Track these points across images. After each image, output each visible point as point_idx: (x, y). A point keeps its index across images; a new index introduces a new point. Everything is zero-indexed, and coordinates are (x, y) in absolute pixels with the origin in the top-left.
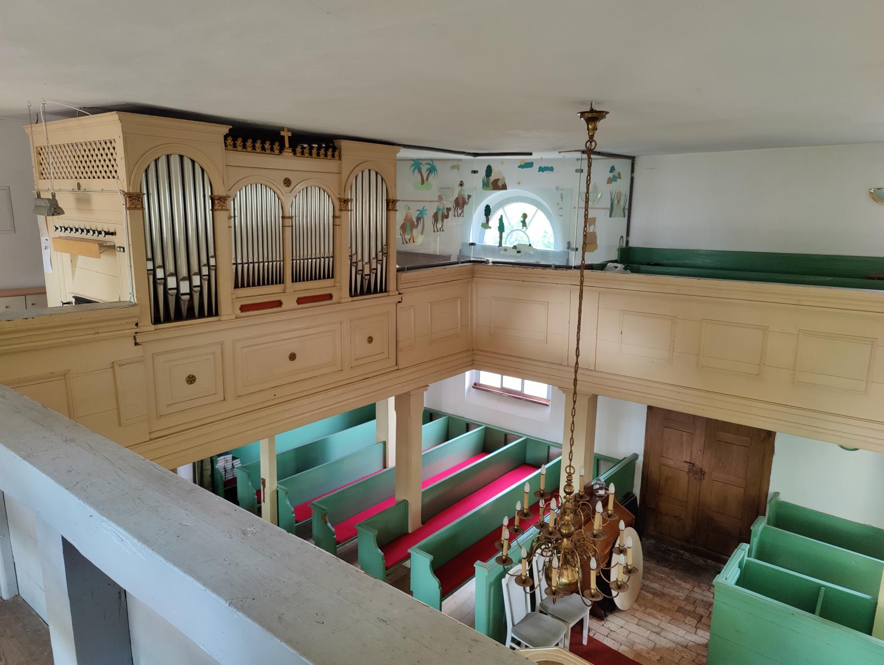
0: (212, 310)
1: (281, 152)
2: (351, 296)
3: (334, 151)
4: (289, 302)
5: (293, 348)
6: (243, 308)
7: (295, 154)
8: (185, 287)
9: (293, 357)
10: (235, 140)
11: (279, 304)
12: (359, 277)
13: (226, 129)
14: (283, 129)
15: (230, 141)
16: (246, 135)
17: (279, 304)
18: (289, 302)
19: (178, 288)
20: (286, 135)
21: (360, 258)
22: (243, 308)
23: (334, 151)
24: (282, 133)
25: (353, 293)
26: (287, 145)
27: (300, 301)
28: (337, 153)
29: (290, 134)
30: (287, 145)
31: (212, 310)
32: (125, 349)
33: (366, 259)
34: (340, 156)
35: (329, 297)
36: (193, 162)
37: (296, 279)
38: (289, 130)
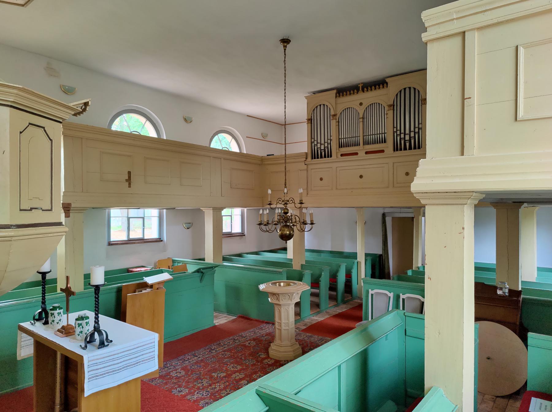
2: (394, 151)
3: (383, 85)
4: (362, 154)
5: (361, 172)
7: (364, 92)
8: (322, 148)
9: (361, 177)
12: (403, 142)
13: (335, 91)
14: (359, 84)
15: (338, 95)
16: (341, 91)
17: (356, 154)
18: (362, 154)
20: (360, 86)
21: (402, 131)
22: (342, 155)
23: (383, 85)
25: (396, 148)
27: (367, 153)
28: (385, 85)
33: (407, 132)
35: (382, 151)
37: (366, 143)
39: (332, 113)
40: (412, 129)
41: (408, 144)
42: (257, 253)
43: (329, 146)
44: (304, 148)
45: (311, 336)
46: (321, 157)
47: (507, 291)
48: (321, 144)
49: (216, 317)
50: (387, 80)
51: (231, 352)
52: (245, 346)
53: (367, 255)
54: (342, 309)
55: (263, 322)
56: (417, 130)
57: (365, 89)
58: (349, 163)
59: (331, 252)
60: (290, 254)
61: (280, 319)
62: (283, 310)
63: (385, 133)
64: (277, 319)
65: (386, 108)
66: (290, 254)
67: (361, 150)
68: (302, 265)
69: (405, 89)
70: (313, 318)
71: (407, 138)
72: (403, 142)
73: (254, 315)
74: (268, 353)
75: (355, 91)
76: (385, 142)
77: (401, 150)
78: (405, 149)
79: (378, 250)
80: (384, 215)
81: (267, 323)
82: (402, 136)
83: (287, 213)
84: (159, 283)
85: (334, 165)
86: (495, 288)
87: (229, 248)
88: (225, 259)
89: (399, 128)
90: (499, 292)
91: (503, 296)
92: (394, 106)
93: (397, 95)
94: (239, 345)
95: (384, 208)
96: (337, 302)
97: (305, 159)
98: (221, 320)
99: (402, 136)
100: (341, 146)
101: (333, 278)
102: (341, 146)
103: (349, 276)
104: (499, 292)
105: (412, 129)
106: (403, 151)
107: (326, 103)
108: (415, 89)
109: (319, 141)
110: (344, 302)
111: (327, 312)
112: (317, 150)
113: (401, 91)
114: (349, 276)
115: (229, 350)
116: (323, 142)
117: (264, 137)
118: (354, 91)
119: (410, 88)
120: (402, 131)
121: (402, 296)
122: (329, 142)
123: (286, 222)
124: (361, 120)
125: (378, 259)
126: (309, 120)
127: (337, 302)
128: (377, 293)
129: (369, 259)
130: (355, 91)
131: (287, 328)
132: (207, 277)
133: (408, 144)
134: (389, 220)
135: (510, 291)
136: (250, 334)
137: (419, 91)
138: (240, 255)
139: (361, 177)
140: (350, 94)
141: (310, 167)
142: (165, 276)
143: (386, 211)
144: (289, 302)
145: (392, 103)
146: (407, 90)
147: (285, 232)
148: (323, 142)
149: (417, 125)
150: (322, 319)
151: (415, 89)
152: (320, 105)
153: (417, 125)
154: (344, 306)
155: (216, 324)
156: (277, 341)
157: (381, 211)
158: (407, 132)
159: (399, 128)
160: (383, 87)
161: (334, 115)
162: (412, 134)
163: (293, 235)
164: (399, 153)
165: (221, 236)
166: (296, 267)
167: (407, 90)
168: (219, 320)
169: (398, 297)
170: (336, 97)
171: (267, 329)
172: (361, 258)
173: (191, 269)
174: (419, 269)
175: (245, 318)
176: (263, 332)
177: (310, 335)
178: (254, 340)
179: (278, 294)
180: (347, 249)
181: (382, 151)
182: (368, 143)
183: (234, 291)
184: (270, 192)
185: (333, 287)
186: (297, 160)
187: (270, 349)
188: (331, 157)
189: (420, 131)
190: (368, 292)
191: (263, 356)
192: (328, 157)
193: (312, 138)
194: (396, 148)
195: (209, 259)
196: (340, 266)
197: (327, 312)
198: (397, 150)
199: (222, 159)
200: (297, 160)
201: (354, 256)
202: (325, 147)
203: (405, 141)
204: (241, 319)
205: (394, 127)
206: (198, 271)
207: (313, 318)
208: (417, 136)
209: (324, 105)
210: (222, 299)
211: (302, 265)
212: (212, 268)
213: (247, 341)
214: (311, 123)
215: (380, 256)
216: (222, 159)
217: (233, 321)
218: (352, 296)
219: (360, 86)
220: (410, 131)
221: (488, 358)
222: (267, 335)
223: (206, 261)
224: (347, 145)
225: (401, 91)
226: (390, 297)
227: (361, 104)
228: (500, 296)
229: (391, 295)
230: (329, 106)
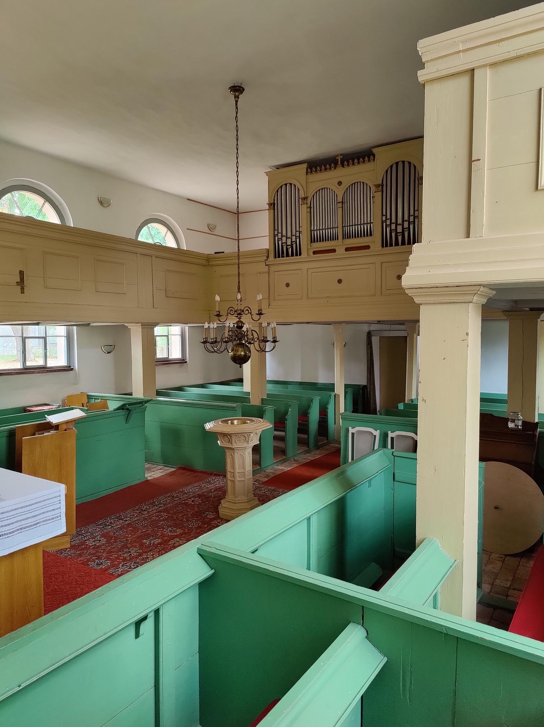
0: (299, 253)
1: (335, 168)
2: (383, 247)
3: (369, 158)
4: (340, 251)
6: (315, 253)
7: (343, 167)
8: (289, 243)
10: (311, 169)
11: (334, 251)
12: (393, 234)
13: (305, 165)
14: (338, 156)
15: (309, 170)
16: (315, 165)
17: (334, 251)
18: (340, 251)
19: (286, 243)
20: (339, 158)
21: (394, 220)
23: (369, 158)
24: (337, 158)
25: (385, 244)
26: (339, 163)
27: (347, 249)
28: (372, 157)
29: (342, 157)
30: (339, 163)
31: (299, 253)
32: (263, 268)
33: (400, 221)
34: (374, 160)
35: (368, 247)
36: (295, 186)
37: (347, 236)
38: (341, 155)
39: (302, 195)
40: (406, 218)
41: (400, 238)
42: (202, 386)
43: (298, 240)
44: (265, 243)
45: (274, 490)
46: (288, 255)
47: (520, 423)
48: (287, 238)
49: (149, 469)
50: (374, 151)
51: (169, 513)
52: (186, 504)
53: (346, 386)
54: (315, 455)
55: (211, 474)
56: (412, 219)
57: (346, 163)
58: (325, 263)
59: (301, 384)
60: (247, 387)
61: (233, 468)
62: (237, 456)
63: (371, 223)
64: (229, 468)
65: (373, 189)
66: (247, 387)
67: (339, 245)
68: (263, 400)
69: (397, 163)
70: (277, 467)
71: (400, 229)
72: (393, 234)
73: (199, 464)
74: (218, 512)
75: (333, 165)
76: (371, 235)
77: (391, 245)
78: (397, 244)
79: (362, 381)
80: (369, 335)
81: (216, 475)
82: (393, 227)
83: (242, 327)
84: (67, 422)
85: (305, 266)
86: (507, 420)
87: (165, 378)
88: (159, 393)
89: (388, 217)
90: (511, 425)
91: (515, 430)
92: (383, 186)
93: (387, 171)
94: (180, 504)
95: (369, 323)
96: (308, 447)
97: (265, 258)
98: (155, 473)
99: (393, 227)
100: (313, 240)
101: (304, 415)
102: (313, 240)
103: (323, 413)
104: (511, 425)
105: (406, 218)
106: (394, 247)
107: (294, 182)
108: (410, 163)
109: (284, 233)
110: (318, 447)
111: (295, 460)
112: (282, 246)
113: (391, 166)
114: (323, 413)
115: (166, 510)
116: (289, 235)
117: (211, 228)
118: (330, 165)
119: (403, 162)
120: (394, 220)
121: (390, 435)
122: (298, 235)
123: (240, 339)
124: (340, 205)
125: (361, 392)
126: (271, 204)
127: (308, 447)
128: (359, 432)
129: (350, 390)
130: (333, 165)
131: (243, 479)
132: (134, 416)
133: (400, 238)
134: (375, 340)
135: (524, 422)
136: (193, 489)
137: (415, 167)
138: (180, 389)
139: (340, 281)
140: (326, 169)
141: (273, 268)
142: (77, 413)
143: (374, 327)
144: (245, 445)
145: (381, 183)
146: (400, 165)
147: (239, 353)
148: (289, 235)
149: (412, 213)
150: (289, 469)
151: (410, 163)
152: (286, 185)
153: (412, 213)
154: (318, 452)
155: (149, 478)
156: (230, 496)
157: (366, 328)
158: (400, 221)
159: (388, 217)
160: (369, 160)
161: (305, 198)
162: (406, 225)
163: (249, 357)
164: (388, 250)
165: (153, 363)
166: (255, 401)
167: (400, 165)
168: (153, 473)
169: (385, 435)
170: (307, 173)
171: (218, 482)
172: (340, 390)
173: (113, 405)
174: (412, 402)
175: (187, 469)
176: (212, 487)
177: (272, 488)
178: (199, 496)
179: (230, 435)
180: (322, 379)
181: (368, 247)
182: (349, 237)
183: (172, 434)
184: (217, 298)
185: (303, 428)
186: (256, 259)
187: (220, 507)
188: (300, 255)
189: (416, 220)
190: (347, 430)
191: (211, 516)
192: (296, 255)
193: (275, 230)
194: (385, 244)
195: (138, 393)
196: (312, 400)
197: (295, 460)
198: (387, 246)
199: (154, 258)
200: (256, 259)
201: (330, 387)
202: (292, 242)
203: (397, 233)
204: (181, 471)
205: (383, 215)
206: (122, 408)
207: (277, 467)
208: (411, 226)
209: (291, 184)
210: (156, 446)
211: (263, 400)
212: (141, 403)
213: (190, 498)
214: (274, 209)
215: (365, 387)
216: (154, 258)
217: (171, 474)
218: (327, 439)
219: (339, 158)
220: (403, 221)
221: (496, 508)
222: (216, 489)
223: (134, 396)
224: (321, 239)
225: (391, 166)
226: (375, 436)
227: (340, 183)
228: (512, 430)
229: (377, 433)
230: (298, 185)
